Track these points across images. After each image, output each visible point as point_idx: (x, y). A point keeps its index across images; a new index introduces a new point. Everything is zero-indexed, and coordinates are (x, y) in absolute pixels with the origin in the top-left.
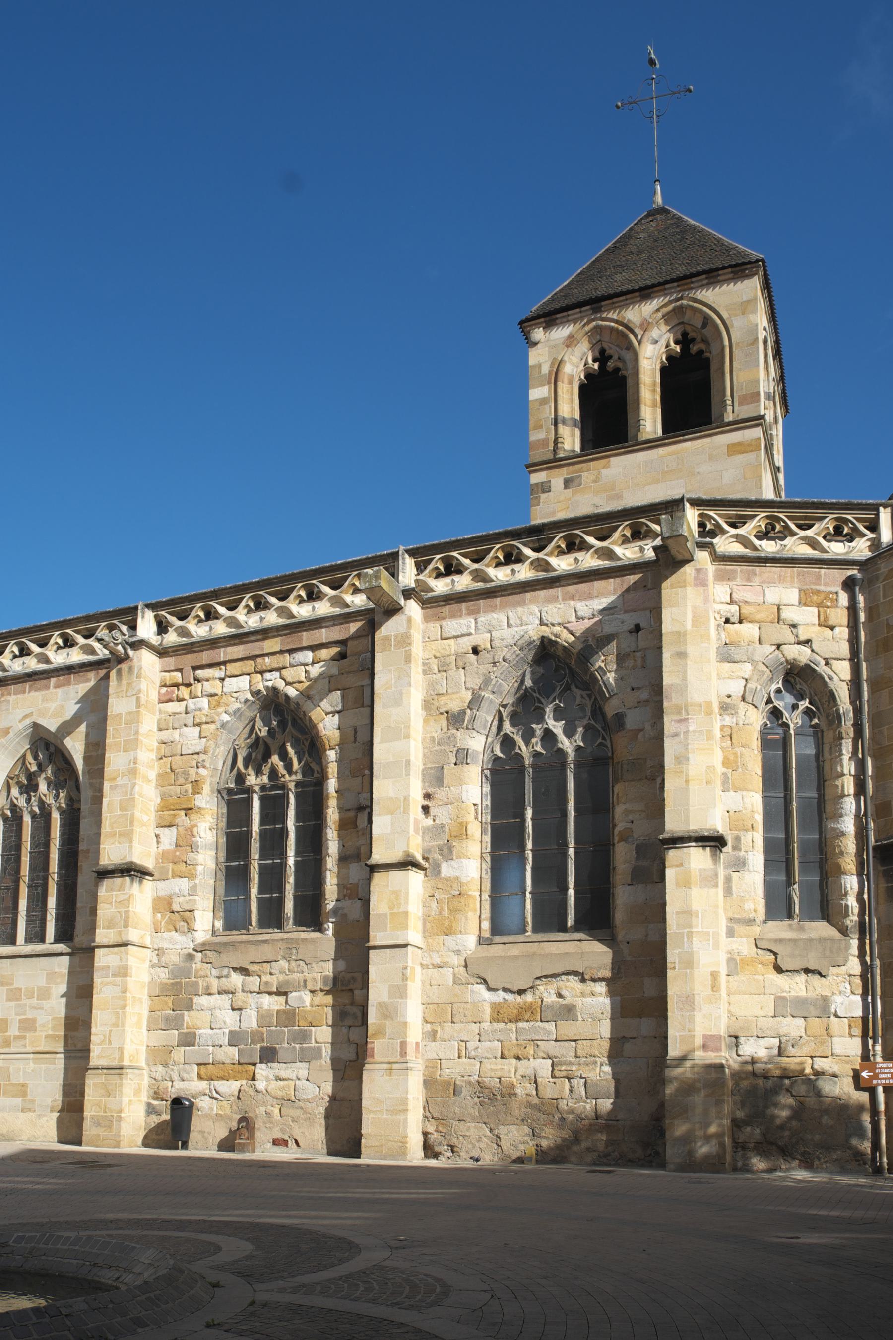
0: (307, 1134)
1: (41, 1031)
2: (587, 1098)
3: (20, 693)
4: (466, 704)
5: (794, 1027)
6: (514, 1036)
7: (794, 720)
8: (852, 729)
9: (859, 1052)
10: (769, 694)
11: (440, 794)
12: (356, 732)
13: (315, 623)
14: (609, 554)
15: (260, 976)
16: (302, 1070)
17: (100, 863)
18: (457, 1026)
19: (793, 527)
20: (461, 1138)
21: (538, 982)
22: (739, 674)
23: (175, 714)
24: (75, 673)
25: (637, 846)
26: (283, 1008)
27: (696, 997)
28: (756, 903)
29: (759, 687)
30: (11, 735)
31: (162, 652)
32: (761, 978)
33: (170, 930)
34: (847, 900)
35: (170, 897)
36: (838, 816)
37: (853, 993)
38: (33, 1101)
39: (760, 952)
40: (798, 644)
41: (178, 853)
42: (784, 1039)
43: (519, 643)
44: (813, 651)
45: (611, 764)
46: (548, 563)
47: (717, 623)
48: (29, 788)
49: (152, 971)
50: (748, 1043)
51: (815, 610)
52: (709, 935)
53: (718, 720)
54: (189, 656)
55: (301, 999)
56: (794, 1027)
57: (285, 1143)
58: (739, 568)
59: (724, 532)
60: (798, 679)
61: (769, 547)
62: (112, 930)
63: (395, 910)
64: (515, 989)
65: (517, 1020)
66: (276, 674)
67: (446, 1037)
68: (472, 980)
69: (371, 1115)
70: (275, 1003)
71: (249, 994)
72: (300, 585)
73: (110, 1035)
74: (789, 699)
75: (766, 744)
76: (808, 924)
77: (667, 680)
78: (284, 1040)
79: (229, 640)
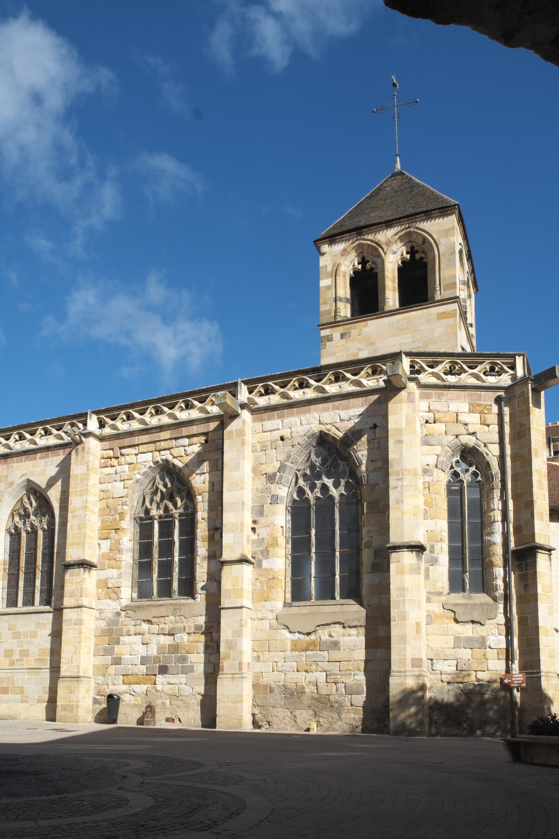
0: (185, 715)
1: (32, 656)
2: (346, 694)
4: (277, 469)
5: (465, 654)
6: (304, 659)
7: (466, 478)
8: (500, 483)
9: (504, 668)
10: (452, 464)
11: (262, 521)
12: (213, 485)
13: (190, 423)
14: (358, 383)
15: (158, 625)
16: (182, 678)
17: (66, 560)
18: (272, 654)
19: (465, 367)
20: (274, 717)
21: (318, 628)
22: (434, 452)
23: (109, 474)
24: (51, 451)
25: (375, 551)
26: (172, 643)
27: (407, 636)
28: (444, 583)
29: (445, 460)
30: (14, 486)
31: (102, 439)
32: (446, 626)
33: (106, 599)
34: (497, 581)
35: (107, 579)
36: (491, 533)
37: (499, 634)
38: (27, 697)
39: (445, 611)
40: (469, 434)
41: (111, 554)
42: (459, 661)
43: (307, 435)
44: (477, 439)
45: (360, 503)
46: (324, 389)
47: (421, 423)
48: (25, 516)
49: (96, 622)
50: (439, 663)
51: (479, 415)
52: (415, 601)
53: (422, 479)
54: (117, 441)
55: (182, 638)
56: (465, 654)
57: (173, 720)
58: (433, 392)
59: (425, 371)
60: (468, 455)
61: (452, 379)
62: (73, 599)
63: (236, 587)
64: (305, 632)
65: (306, 650)
66: (168, 452)
67: (265, 660)
68: (280, 627)
69: (222, 704)
70: (167, 640)
71: (152, 635)
72: (181, 400)
73: (72, 659)
74: (464, 466)
75: (450, 492)
76: (474, 595)
77: (392, 456)
78: (172, 661)
79: (141, 432)
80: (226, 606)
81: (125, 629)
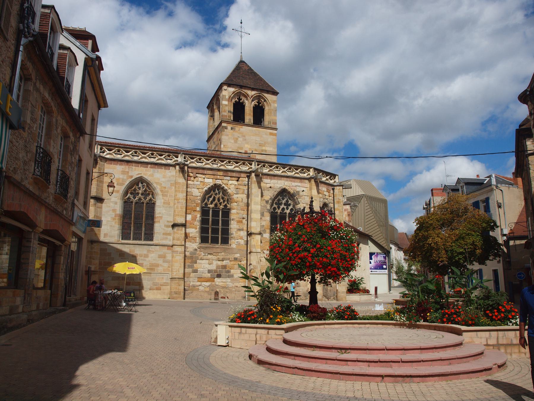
3: (137, 166)
11: (263, 218)
16: (229, 280)
33: (189, 242)
57: (224, 298)
80: (253, 251)
81: (200, 257)
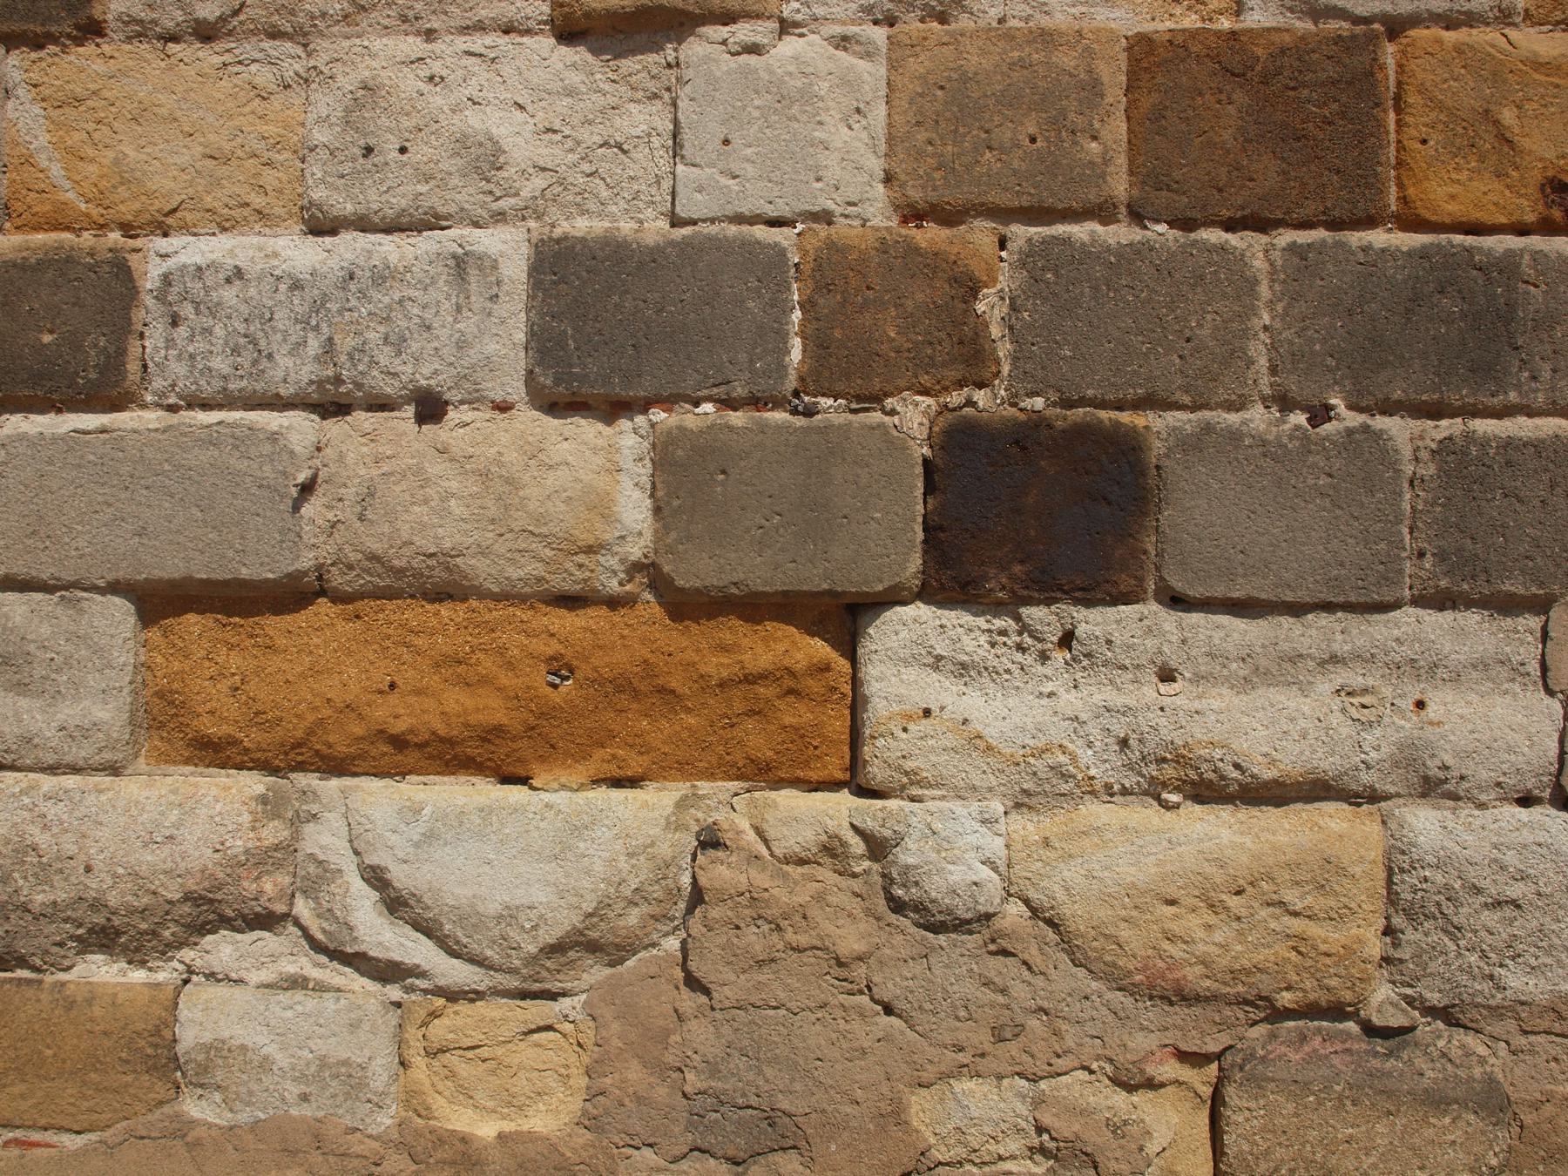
78: (1235, 356)
